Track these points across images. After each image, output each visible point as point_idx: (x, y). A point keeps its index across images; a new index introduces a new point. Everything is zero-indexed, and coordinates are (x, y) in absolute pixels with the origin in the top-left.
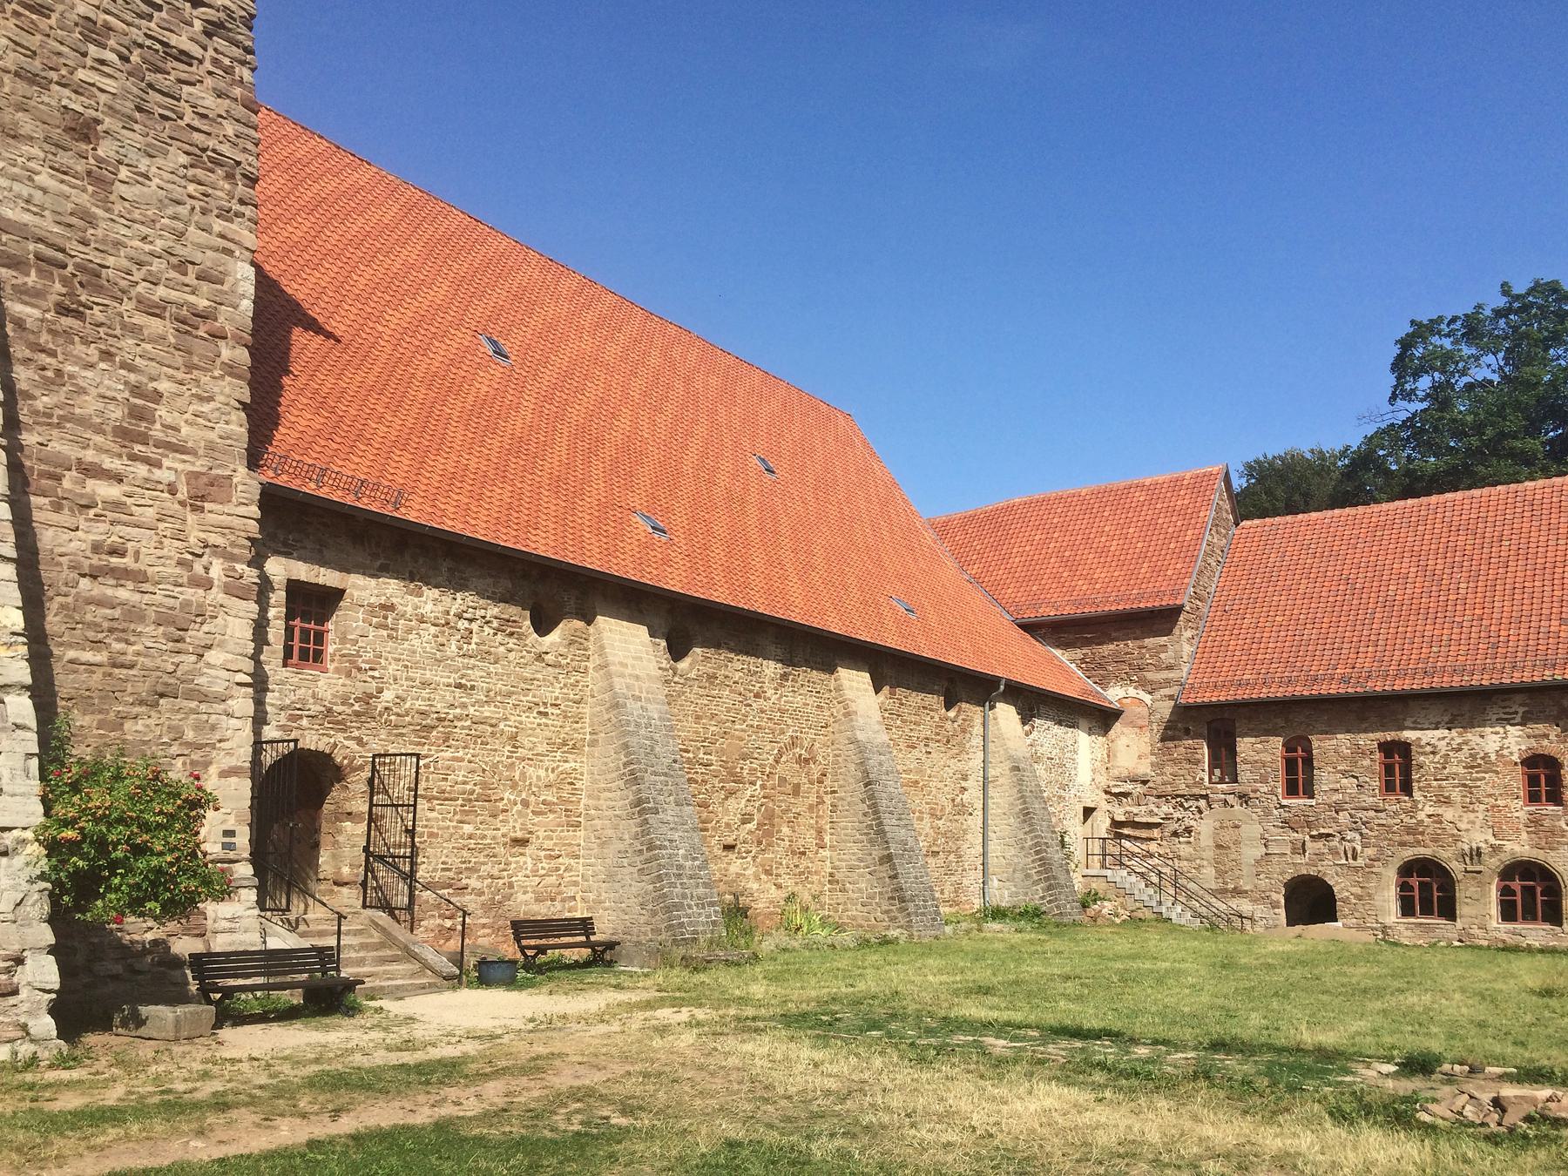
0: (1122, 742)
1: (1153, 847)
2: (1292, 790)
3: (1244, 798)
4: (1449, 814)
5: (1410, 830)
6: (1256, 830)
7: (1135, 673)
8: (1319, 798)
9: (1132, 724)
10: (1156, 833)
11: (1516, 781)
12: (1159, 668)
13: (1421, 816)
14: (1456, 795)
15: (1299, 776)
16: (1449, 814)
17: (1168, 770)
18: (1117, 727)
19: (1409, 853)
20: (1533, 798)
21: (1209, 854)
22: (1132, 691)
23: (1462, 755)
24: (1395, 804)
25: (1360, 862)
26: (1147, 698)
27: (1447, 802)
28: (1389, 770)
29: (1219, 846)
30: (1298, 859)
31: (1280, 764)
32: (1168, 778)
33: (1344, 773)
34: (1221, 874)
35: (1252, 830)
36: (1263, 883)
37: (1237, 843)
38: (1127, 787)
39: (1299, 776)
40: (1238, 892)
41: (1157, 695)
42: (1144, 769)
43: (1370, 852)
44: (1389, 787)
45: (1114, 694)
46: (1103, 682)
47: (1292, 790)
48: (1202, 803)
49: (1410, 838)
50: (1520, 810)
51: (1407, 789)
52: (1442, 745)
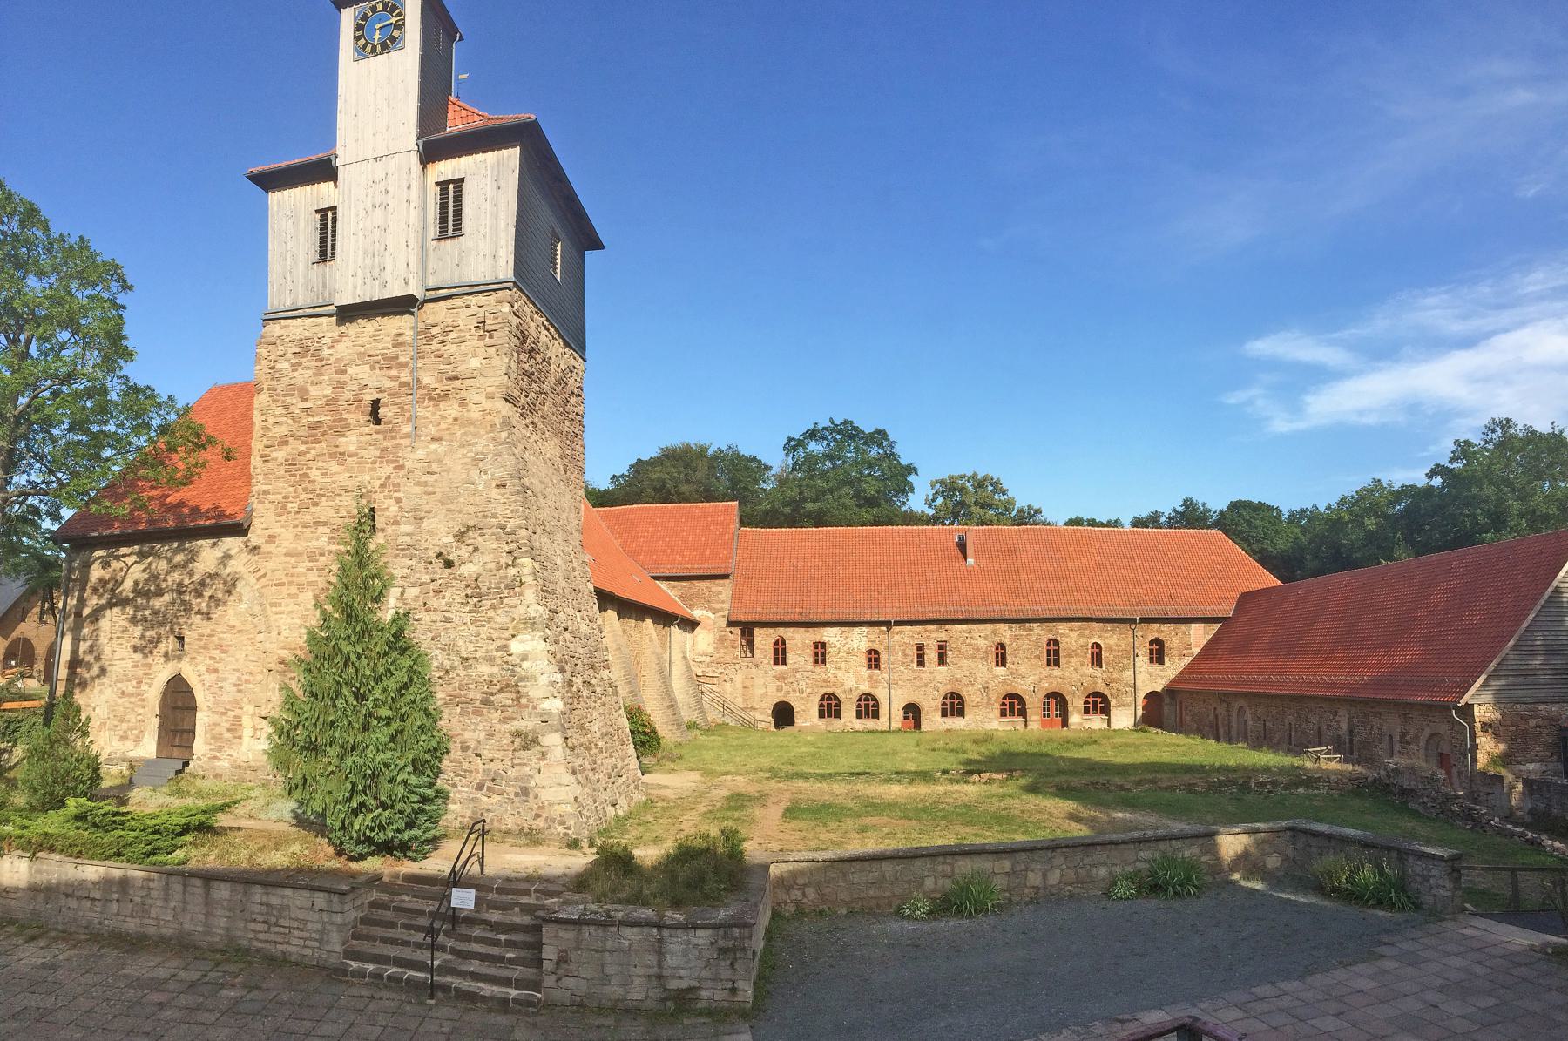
0: (700, 637)
1: (714, 688)
2: (776, 663)
3: (757, 666)
4: (840, 674)
5: (825, 681)
6: (762, 681)
7: (707, 604)
8: (789, 666)
9: (705, 628)
10: (715, 680)
11: (863, 660)
12: (718, 602)
13: (829, 674)
14: (843, 665)
15: (780, 656)
16: (840, 674)
17: (722, 651)
18: (698, 630)
19: (824, 691)
20: (869, 667)
21: (740, 691)
22: (705, 613)
23: (845, 648)
24: (819, 668)
25: (804, 695)
26: (713, 616)
27: (840, 668)
28: (816, 654)
29: (745, 687)
30: (780, 694)
31: (772, 651)
32: (722, 655)
33: (799, 655)
34: (745, 700)
35: (759, 681)
36: (764, 705)
37: (753, 685)
38: (703, 658)
39: (780, 656)
40: (753, 708)
41: (717, 615)
42: (711, 650)
43: (809, 690)
44: (816, 662)
45: (697, 614)
46: (691, 607)
47: (776, 663)
48: (737, 666)
49: (824, 684)
50: (865, 672)
51: (824, 662)
52: (838, 644)
